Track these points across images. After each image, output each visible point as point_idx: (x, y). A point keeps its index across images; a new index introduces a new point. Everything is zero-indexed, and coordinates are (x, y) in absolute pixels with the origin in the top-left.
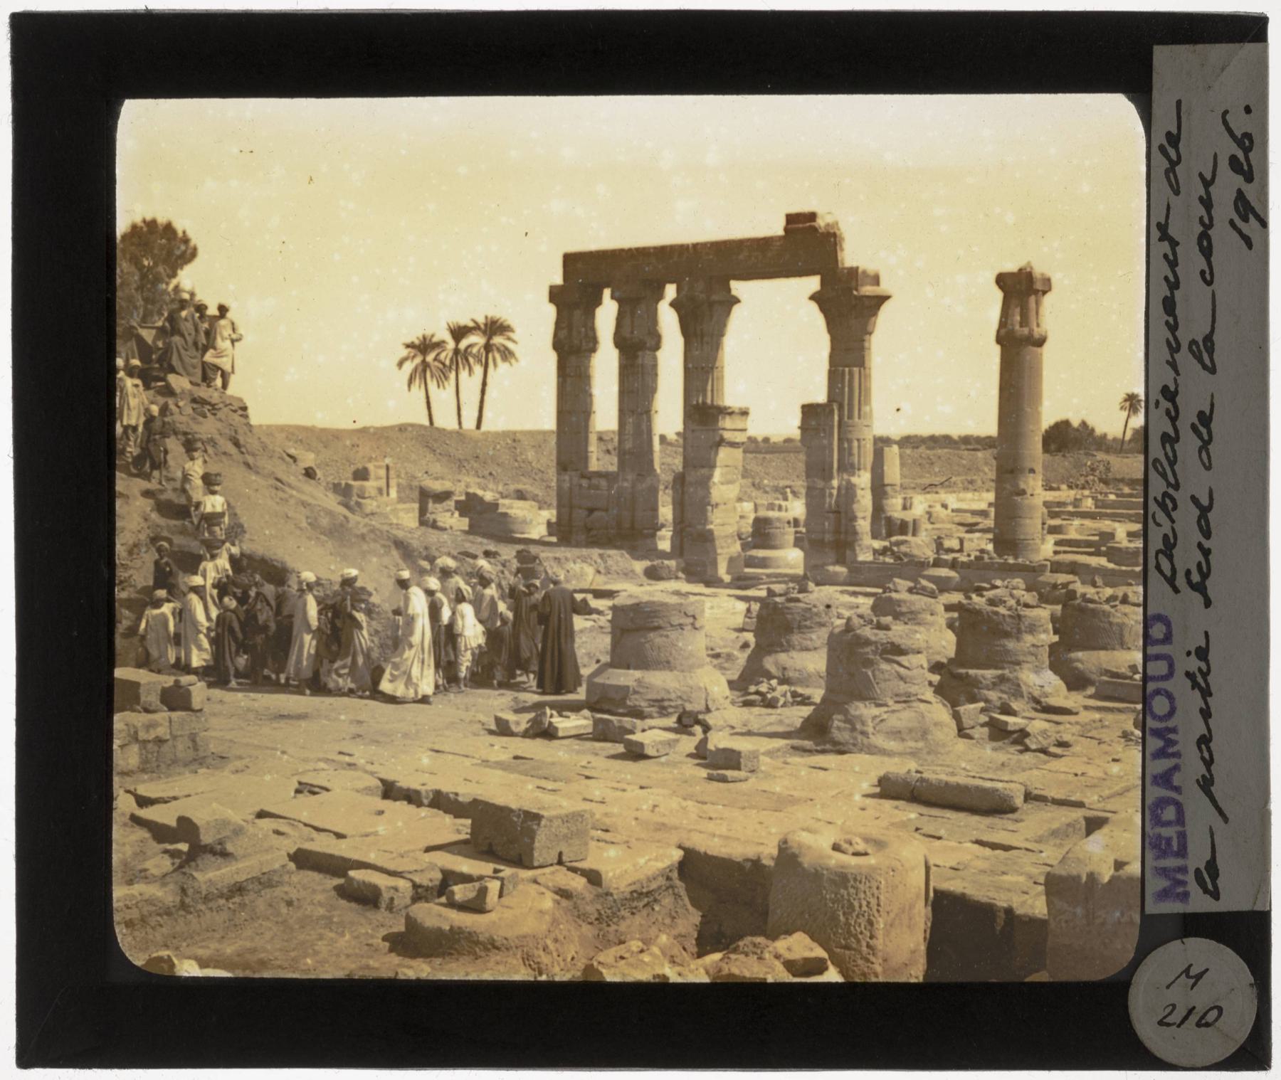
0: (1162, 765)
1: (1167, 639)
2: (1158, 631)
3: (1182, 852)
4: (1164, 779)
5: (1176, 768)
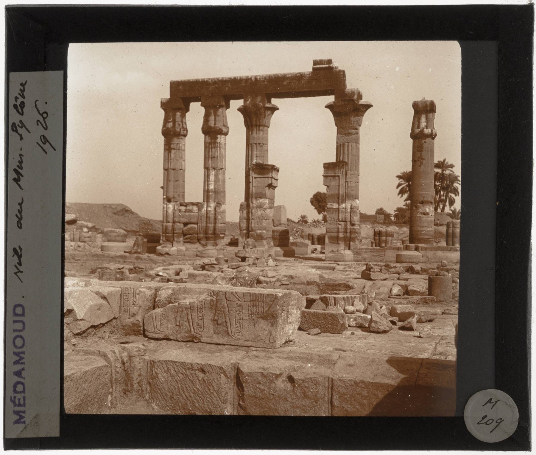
0: (18, 367)
1: (23, 315)
2: (19, 310)
3: (24, 405)
4: (18, 374)
5: (23, 369)
